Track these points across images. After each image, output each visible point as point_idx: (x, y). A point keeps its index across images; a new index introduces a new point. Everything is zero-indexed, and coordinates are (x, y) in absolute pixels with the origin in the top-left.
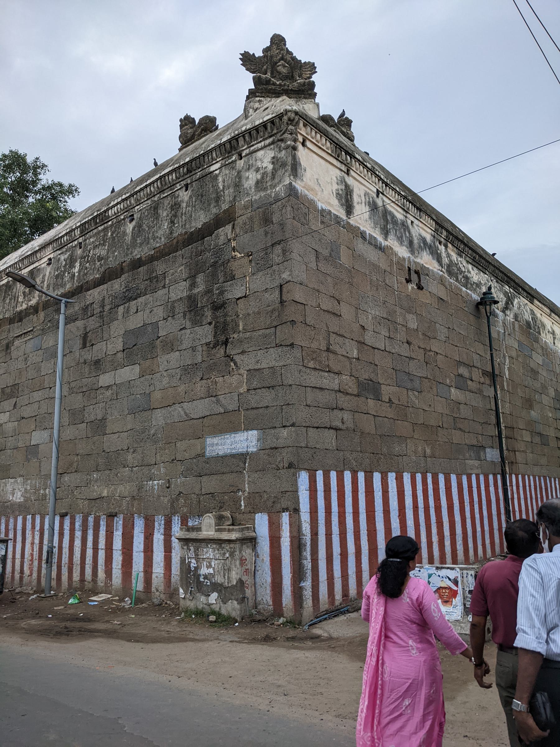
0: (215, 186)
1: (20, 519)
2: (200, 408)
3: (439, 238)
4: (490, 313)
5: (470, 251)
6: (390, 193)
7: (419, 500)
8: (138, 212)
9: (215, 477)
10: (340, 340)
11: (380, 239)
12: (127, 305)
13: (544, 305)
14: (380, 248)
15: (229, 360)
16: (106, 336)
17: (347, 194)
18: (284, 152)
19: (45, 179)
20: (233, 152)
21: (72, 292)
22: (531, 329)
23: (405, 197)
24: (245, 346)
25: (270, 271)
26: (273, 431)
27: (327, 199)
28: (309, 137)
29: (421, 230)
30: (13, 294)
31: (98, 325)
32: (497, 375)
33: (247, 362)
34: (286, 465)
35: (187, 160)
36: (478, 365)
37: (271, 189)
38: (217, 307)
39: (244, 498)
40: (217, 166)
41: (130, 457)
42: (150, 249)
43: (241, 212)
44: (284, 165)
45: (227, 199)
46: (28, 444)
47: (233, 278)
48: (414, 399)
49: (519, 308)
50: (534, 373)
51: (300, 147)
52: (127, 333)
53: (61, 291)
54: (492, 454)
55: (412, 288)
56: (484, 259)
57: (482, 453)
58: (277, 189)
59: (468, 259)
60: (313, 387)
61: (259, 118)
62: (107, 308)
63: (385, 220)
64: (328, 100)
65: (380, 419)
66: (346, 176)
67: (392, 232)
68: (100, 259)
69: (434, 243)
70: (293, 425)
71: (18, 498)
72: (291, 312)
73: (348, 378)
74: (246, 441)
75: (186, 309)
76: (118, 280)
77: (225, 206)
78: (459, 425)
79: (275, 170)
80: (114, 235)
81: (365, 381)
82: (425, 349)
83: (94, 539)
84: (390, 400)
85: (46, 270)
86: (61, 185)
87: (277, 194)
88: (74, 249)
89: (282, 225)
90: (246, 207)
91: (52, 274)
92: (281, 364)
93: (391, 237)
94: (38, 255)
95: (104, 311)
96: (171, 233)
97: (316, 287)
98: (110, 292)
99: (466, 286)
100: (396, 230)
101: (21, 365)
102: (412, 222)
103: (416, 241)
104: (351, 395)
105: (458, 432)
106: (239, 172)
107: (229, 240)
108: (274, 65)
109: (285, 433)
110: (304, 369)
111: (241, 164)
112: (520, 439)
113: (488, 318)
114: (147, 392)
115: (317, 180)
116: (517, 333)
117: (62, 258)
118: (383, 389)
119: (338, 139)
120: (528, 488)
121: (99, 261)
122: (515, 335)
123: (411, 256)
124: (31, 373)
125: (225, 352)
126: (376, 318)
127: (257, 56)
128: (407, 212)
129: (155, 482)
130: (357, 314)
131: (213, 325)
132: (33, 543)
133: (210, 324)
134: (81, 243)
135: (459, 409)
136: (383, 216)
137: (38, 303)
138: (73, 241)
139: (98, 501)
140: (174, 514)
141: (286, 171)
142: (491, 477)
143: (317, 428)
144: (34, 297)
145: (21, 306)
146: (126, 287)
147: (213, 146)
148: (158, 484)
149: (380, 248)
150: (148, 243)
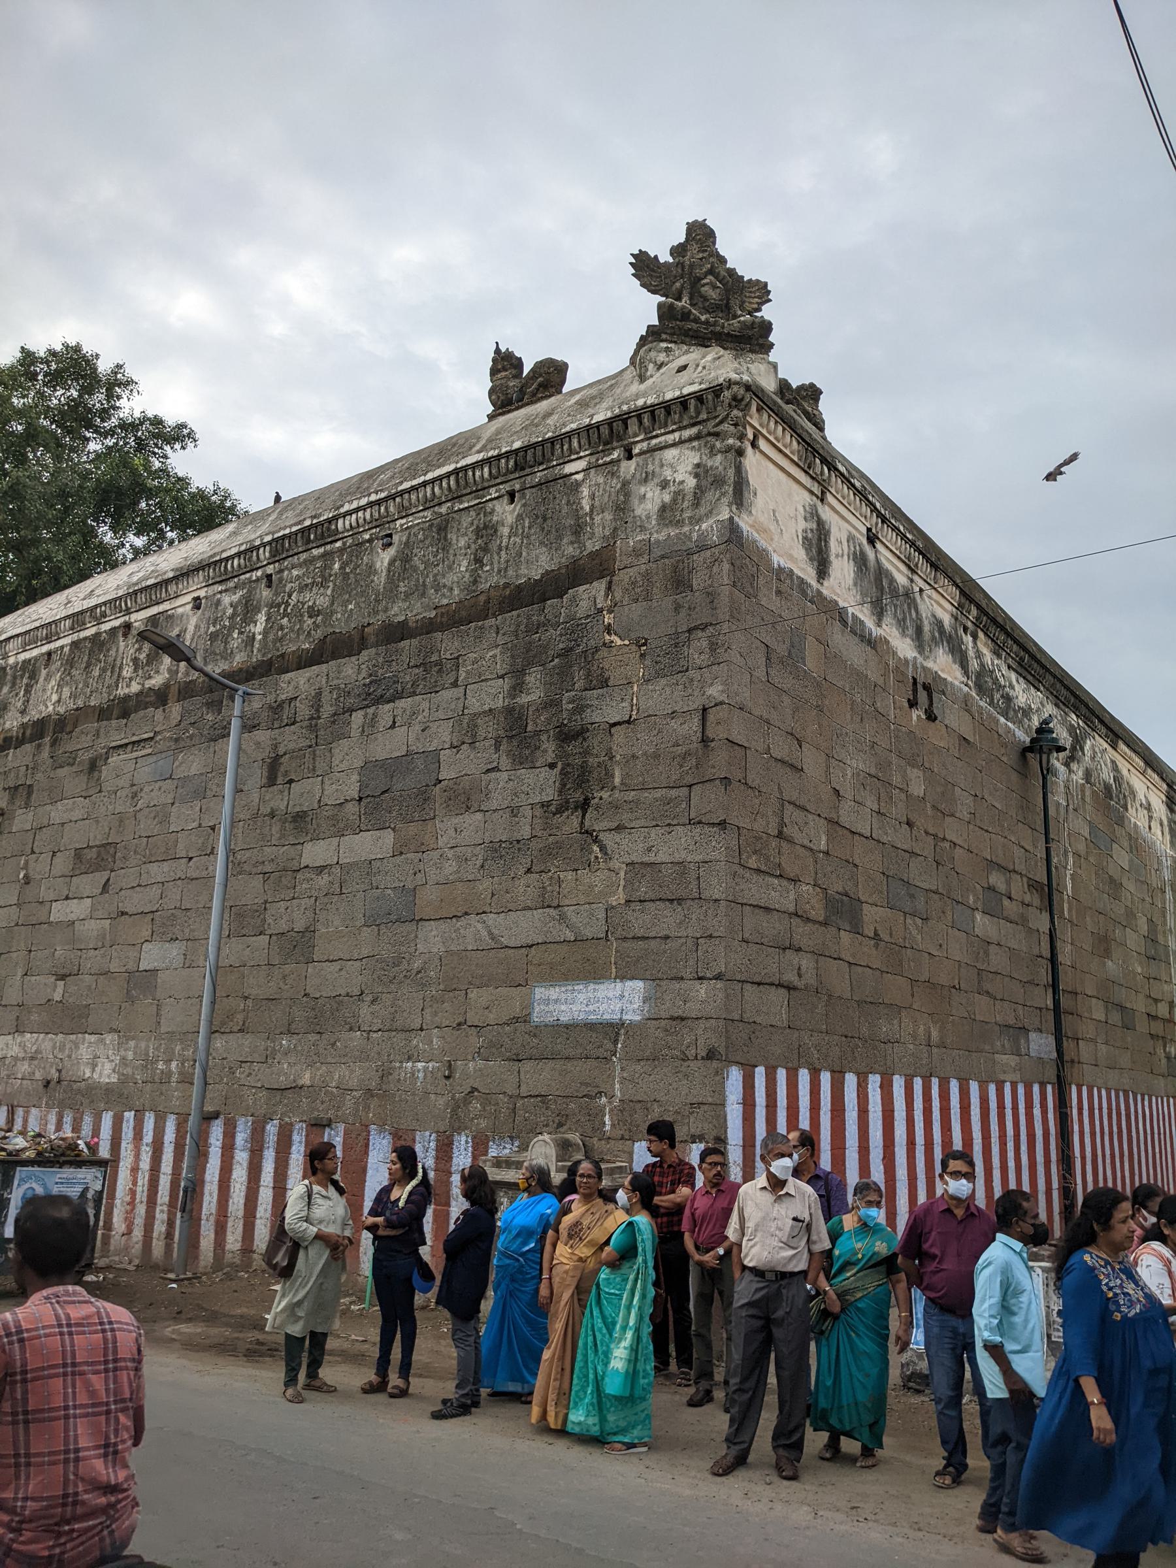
1: (107, 1120)
2: (525, 926)
3: (964, 621)
4: (1048, 770)
6: (887, 535)
7: (917, 1128)
8: (402, 530)
9: (551, 1064)
10: (797, 813)
11: (870, 623)
12: (371, 710)
13: (1135, 751)
14: (869, 642)
15: (589, 840)
16: (321, 766)
17: (820, 539)
18: (719, 457)
19: (130, 406)
20: (615, 444)
21: (247, 671)
22: (1111, 799)
23: (913, 544)
24: (625, 817)
26: (676, 985)
27: (787, 551)
28: (764, 432)
29: (935, 606)
30: (110, 659)
33: (627, 848)
34: (704, 1054)
35: (517, 445)
36: (1020, 867)
37: (691, 524)
38: (568, 735)
39: (611, 1111)
40: (581, 465)
41: (365, 1011)
43: (627, 561)
44: (718, 482)
45: (598, 531)
46: (131, 966)
47: (605, 683)
48: (915, 932)
49: (1093, 758)
51: (749, 450)
53: (223, 666)
54: (1041, 1044)
55: (919, 716)
58: (704, 526)
60: (754, 906)
62: (327, 710)
63: (879, 589)
64: (792, 359)
65: (860, 969)
66: (819, 503)
67: (890, 611)
68: (313, 612)
70: (718, 977)
71: (105, 1074)
72: (720, 761)
74: (618, 1000)
76: (353, 659)
77: (592, 546)
78: (987, 986)
80: (348, 570)
81: (838, 896)
82: (935, 836)
83: (276, 1169)
84: (876, 934)
85: (188, 619)
86: (157, 422)
87: (703, 536)
88: (253, 585)
89: (711, 596)
90: (636, 553)
91: (202, 630)
92: (699, 858)
93: (888, 619)
94: (172, 588)
95: (319, 718)
96: (475, 582)
97: (765, 716)
98: (335, 682)
100: (896, 606)
101: (122, 805)
102: (921, 590)
103: (927, 628)
104: (815, 922)
105: (985, 999)
106: (625, 484)
107: (600, 611)
108: (696, 282)
109: (702, 990)
110: (741, 871)
111: (629, 468)
112: (1086, 1014)
113: (1044, 778)
115: (774, 511)
116: (1088, 807)
118: (865, 912)
119: (810, 435)
120: (1097, 1111)
121: (310, 617)
122: (1085, 811)
124: (147, 825)
125: (582, 823)
126: (858, 775)
127: (662, 261)
128: (913, 571)
129: (420, 1065)
130: (828, 767)
131: (557, 770)
132: (135, 1170)
133: (552, 766)
134: (269, 577)
135: (987, 953)
136: (875, 580)
137: (167, 686)
138: (252, 571)
139: (289, 1094)
140: (459, 1130)
141: (723, 494)
142: (1036, 1088)
143: (759, 984)
144: (158, 672)
145: (128, 686)
146: (371, 675)
147: (574, 426)
148: (425, 1069)
150: (423, 595)
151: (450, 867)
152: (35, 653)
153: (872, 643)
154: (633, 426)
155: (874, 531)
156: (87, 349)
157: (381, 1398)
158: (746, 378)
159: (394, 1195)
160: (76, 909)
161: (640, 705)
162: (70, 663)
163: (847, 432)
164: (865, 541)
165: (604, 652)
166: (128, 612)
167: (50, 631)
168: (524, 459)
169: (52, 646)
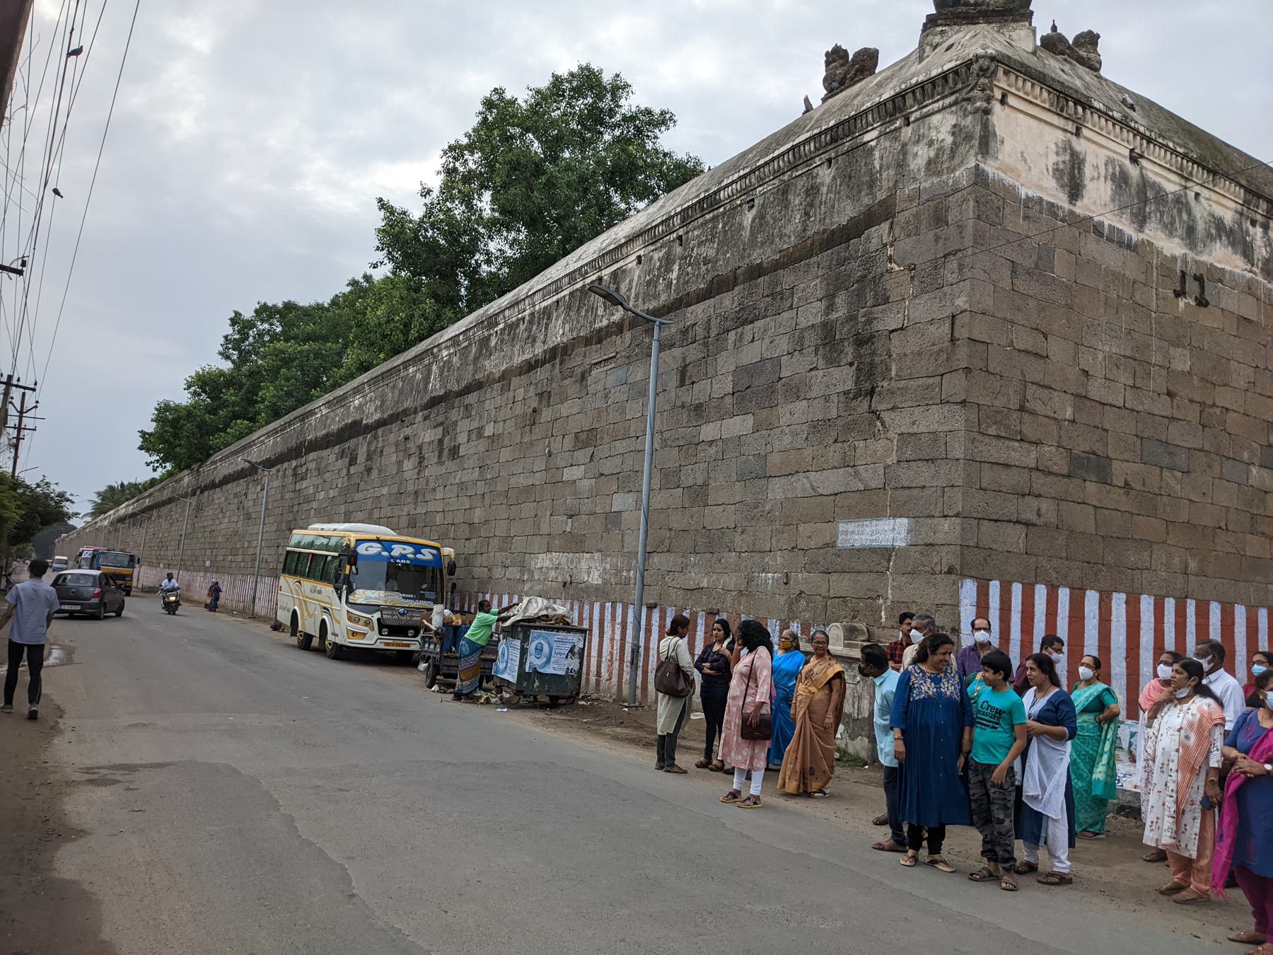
1: (597, 606)
2: (832, 481)
6: (1156, 153)
9: (848, 575)
11: (1129, 231)
12: (739, 330)
14: (1129, 246)
16: (711, 372)
17: (1073, 167)
18: (970, 118)
19: (629, 104)
25: (939, 294)
28: (1013, 90)
29: (1214, 206)
33: (898, 422)
35: (832, 123)
40: (874, 134)
41: (737, 539)
42: (774, 252)
43: (903, 206)
44: (969, 138)
45: (885, 184)
46: (608, 510)
47: (886, 301)
51: (997, 107)
52: (739, 371)
53: (652, 305)
55: (1187, 305)
62: (713, 334)
63: (1140, 199)
65: (1106, 512)
66: (1074, 138)
69: (1240, 225)
70: (957, 516)
71: (595, 579)
72: (962, 356)
73: (1053, 449)
74: (890, 532)
75: (819, 342)
77: (881, 196)
79: (955, 145)
82: (1202, 404)
86: (648, 112)
87: (956, 182)
89: (961, 228)
90: (910, 199)
92: (946, 428)
94: (624, 250)
96: (805, 230)
97: (1008, 317)
101: (600, 403)
102: (1197, 195)
103: (1200, 226)
104: (1056, 475)
107: (885, 245)
109: (946, 525)
111: (907, 132)
114: (763, 453)
115: (1022, 153)
117: (656, 256)
123: (1188, 252)
124: (613, 416)
126: (1111, 357)
128: (1187, 179)
132: (612, 639)
133: (851, 364)
134: (680, 238)
137: (622, 320)
141: (971, 147)
143: (996, 521)
147: (869, 105)
149: (1129, 246)
151: (787, 440)
152: (550, 301)
153: (1130, 246)
156: (595, 67)
157: (706, 771)
158: (990, 51)
159: (716, 648)
161: (913, 316)
162: (569, 308)
164: (1127, 162)
165: (887, 277)
167: (556, 286)
168: (848, 128)
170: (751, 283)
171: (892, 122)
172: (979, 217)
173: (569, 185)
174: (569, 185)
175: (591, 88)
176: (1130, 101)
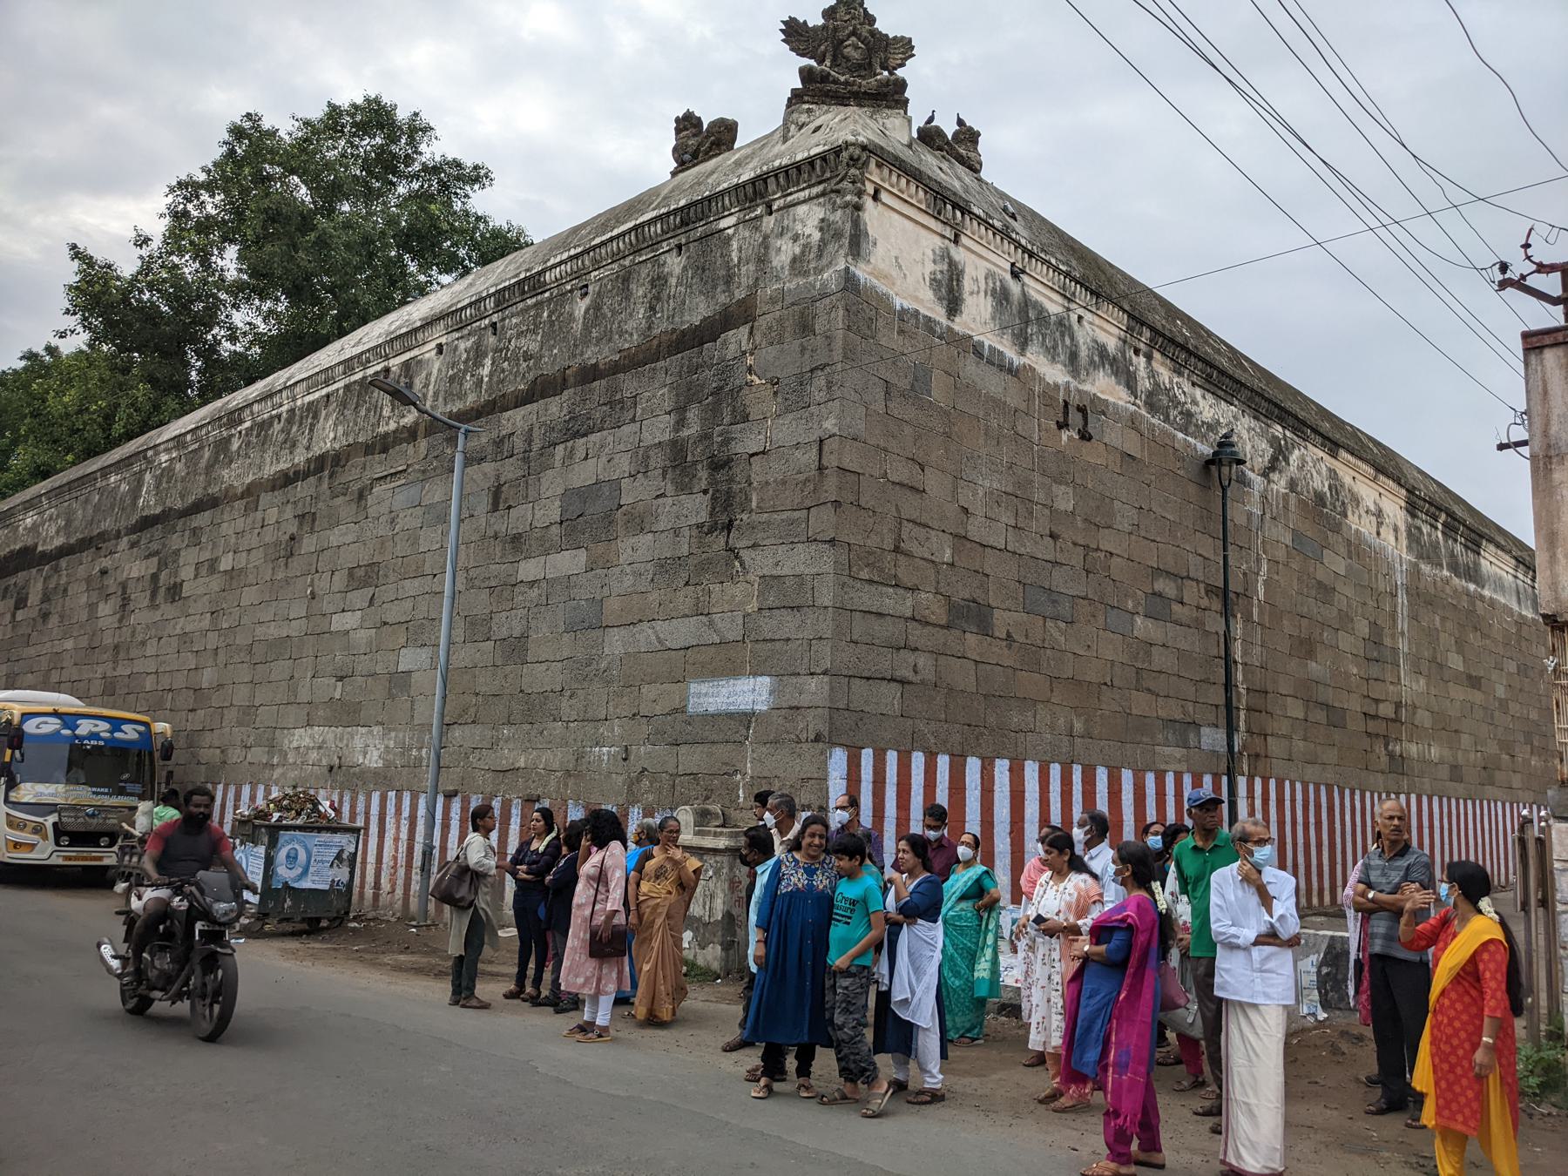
0: (726, 256)
1: (376, 797)
2: (682, 632)
5: (1200, 365)
6: (1037, 269)
11: (1011, 353)
12: (569, 444)
13: (1361, 459)
14: (1010, 371)
16: (532, 494)
18: (839, 212)
19: (431, 151)
22: (1324, 506)
26: (794, 680)
27: (912, 291)
28: (886, 185)
31: (521, 473)
32: (1238, 594)
33: (760, 562)
35: (682, 203)
38: (719, 464)
40: (732, 220)
41: (565, 704)
42: (613, 351)
44: (838, 235)
45: (744, 280)
46: (392, 669)
47: (746, 419)
48: (1056, 634)
50: (1325, 591)
51: (868, 203)
52: (567, 494)
53: (456, 407)
55: (1070, 438)
56: (1230, 377)
57: (1192, 736)
59: (1195, 378)
61: (806, 146)
62: (535, 448)
63: (1023, 320)
69: (1124, 354)
70: (825, 673)
71: (374, 760)
73: (931, 596)
74: (750, 693)
75: (668, 463)
77: (740, 294)
79: (823, 243)
82: (1086, 547)
84: (1009, 635)
86: (457, 164)
90: (773, 300)
94: (420, 336)
96: (649, 328)
97: (882, 444)
99: (1185, 431)
102: (1080, 318)
103: (1083, 353)
107: (744, 353)
108: (838, 45)
109: (813, 684)
111: (769, 222)
117: (462, 345)
120: (1288, 803)
124: (402, 548)
127: (810, 25)
128: (1070, 300)
129: (605, 749)
131: (709, 496)
132: (396, 839)
133: (705, 492)
134: (494, 325)
135: (1149, 654)
137: (416, 423)
140: (633, 803)
143: (868, 679)
147: (725, 185)
149: (1010, 371)
150: (610, 340)
151: (628, 581)
152: (317, 395)
153: (1013, 371)
154: (772, 185)
155: (1019, 265)
156: (386, 100)
158: (861, 139)
159: (534, 846)
160: (348, 621)
161: (775, 438)
162: (344, 405)
163: (1012, 165)
164: (1008, 277)
165: (746, 391)
166: (387, 358)
167: (327, 376)
169: (330, 389)
170: (585, 388)
171: (752, 208)
172: (849, 328)
173: (348, 246)
174: (348, 246)
175: (381, 127)
176: (1011, 209)
